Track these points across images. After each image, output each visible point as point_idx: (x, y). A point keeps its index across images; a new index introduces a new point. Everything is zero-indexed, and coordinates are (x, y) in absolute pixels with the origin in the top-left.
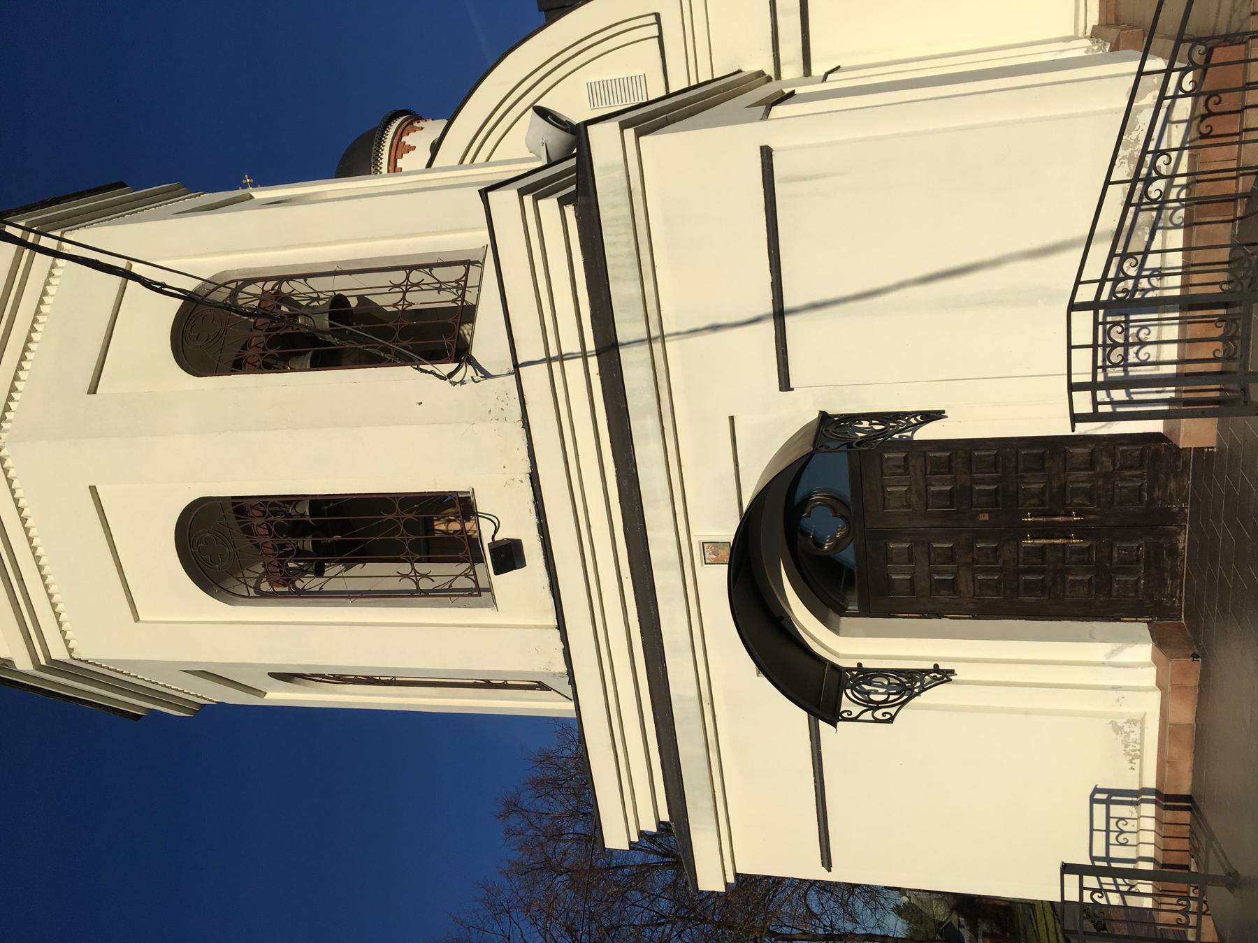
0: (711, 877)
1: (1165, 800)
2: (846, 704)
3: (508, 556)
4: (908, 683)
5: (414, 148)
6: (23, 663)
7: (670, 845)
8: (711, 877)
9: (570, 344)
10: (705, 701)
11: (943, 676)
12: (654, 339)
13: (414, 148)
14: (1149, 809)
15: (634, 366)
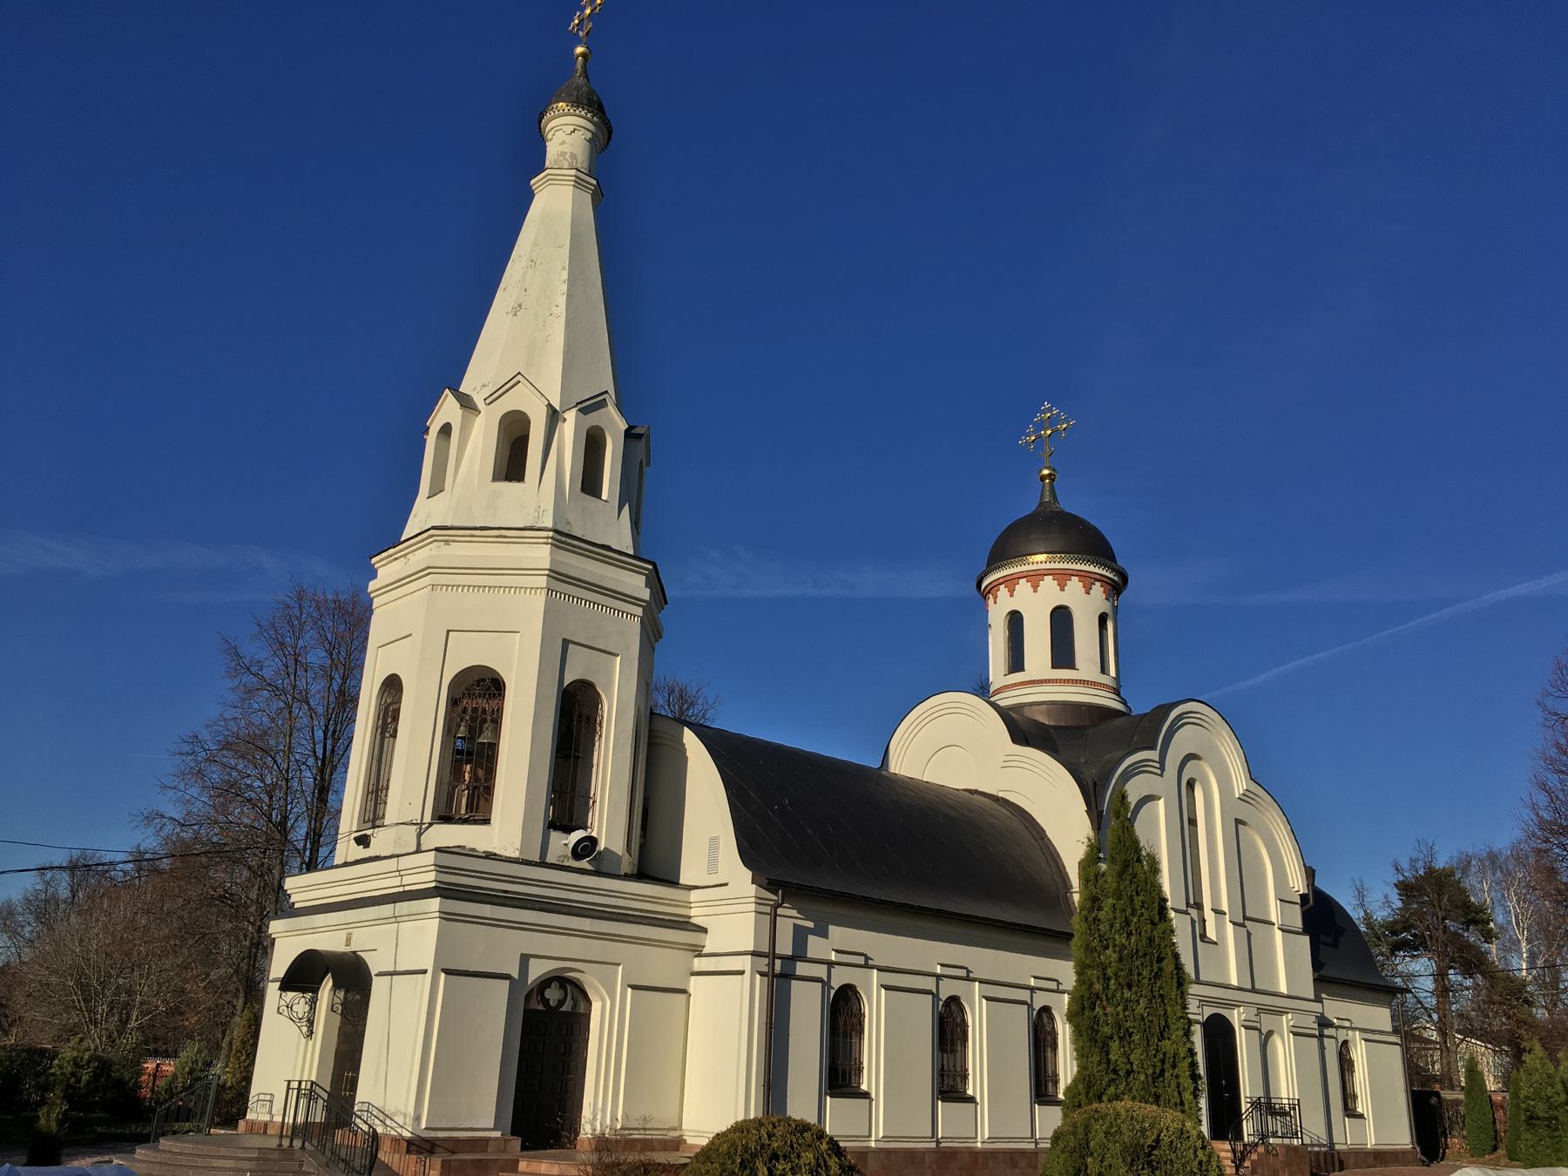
0: (276, 927)
1: (266, 1124)
2: (291, 995)
3: (363, 841)
4: (311, 1023)
5: (1062, 589)
6: (372, 585)
7: (286, 909)
8: (276, 927)
9: (407, 880)
10: (314, 930)
11: (310, 1033)
12: (396, 919)
13: (1062, 589)
14: (267, 1118)
15: (387, 910)
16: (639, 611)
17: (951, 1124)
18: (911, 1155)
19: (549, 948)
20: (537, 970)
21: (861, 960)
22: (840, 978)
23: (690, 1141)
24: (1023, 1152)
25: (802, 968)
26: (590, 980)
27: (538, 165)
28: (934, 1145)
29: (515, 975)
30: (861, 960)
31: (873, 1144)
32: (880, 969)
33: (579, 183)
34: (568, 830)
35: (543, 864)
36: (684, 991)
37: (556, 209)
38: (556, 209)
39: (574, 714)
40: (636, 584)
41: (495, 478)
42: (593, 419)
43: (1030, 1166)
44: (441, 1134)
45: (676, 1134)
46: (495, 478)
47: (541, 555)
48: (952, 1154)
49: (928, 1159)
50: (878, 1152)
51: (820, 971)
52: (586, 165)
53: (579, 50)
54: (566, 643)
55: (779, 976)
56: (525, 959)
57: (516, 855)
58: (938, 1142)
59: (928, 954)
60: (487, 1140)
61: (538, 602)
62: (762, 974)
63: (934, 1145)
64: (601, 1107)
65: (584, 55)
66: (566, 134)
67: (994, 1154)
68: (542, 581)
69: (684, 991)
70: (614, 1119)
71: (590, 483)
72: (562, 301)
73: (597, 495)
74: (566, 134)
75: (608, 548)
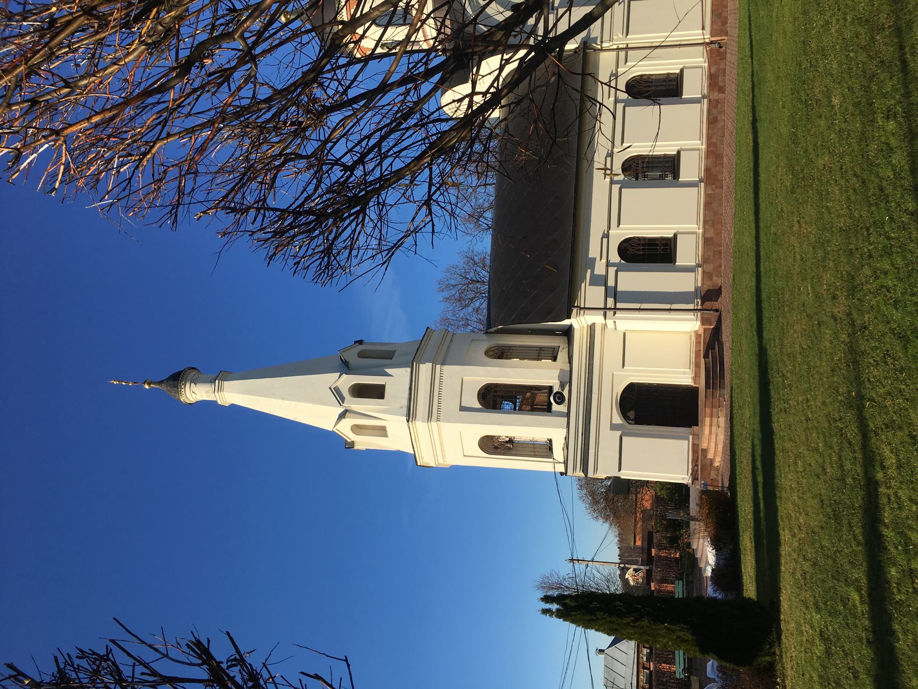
16: (438, 367)
17: (691, 169)
18: (707, 205)
19: (607, 411)
20: (618, 419)
21: (605, 240)
22: (615, 258)
23: (697, 328)
24: (709, 111)
25: (611, 283)
26: (619, 389)
27: (215, 402)
28: (703, 184)
29: (620, 433)
30: (605, 240)
31: (701, 231)
32: (609, 228)
33: (220, 389)
34: (550, 404)
35: (568, 415)
36: (624, 334)
37: (234, 394)
38: (234, 394)
39: (494, 398)
40: (425, 369)
41: (386, 436)
42: (346, 394)
43: (716, 107)
44: (690, 467)
45: (693, 335)
46: (386, 436)
47: (420, 425)
48: (707, 170)
49: (710, 192)
50: (704, 227)
51: (612, 270)
52: (209, 385)
53: (147, 387)
54: (463, 409)
55: (617, 301)
56: (613, 427)
57: (565, 431)
58: (701, 181)
59: (600, 188)
60: (693, 444)
61: (443, 425)
62: (615, 313)
63: (703, 184)
64: (681, 375)
65: (149, 384)
66: (195, 393)
67: (709, 137)
68: (434, 424)
69: (624, 334)
70: (684, 373)
71: (377, 392)
72: (287, 403)
73: (382, 388)
74: (195, 393)
75: (410, 389)
